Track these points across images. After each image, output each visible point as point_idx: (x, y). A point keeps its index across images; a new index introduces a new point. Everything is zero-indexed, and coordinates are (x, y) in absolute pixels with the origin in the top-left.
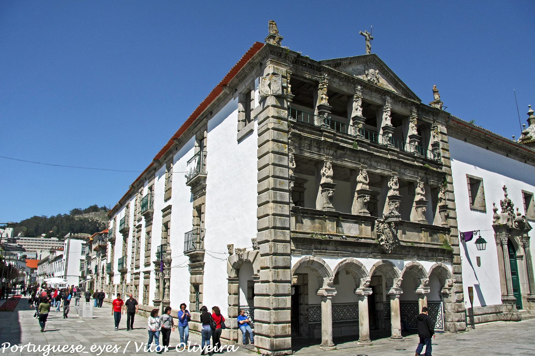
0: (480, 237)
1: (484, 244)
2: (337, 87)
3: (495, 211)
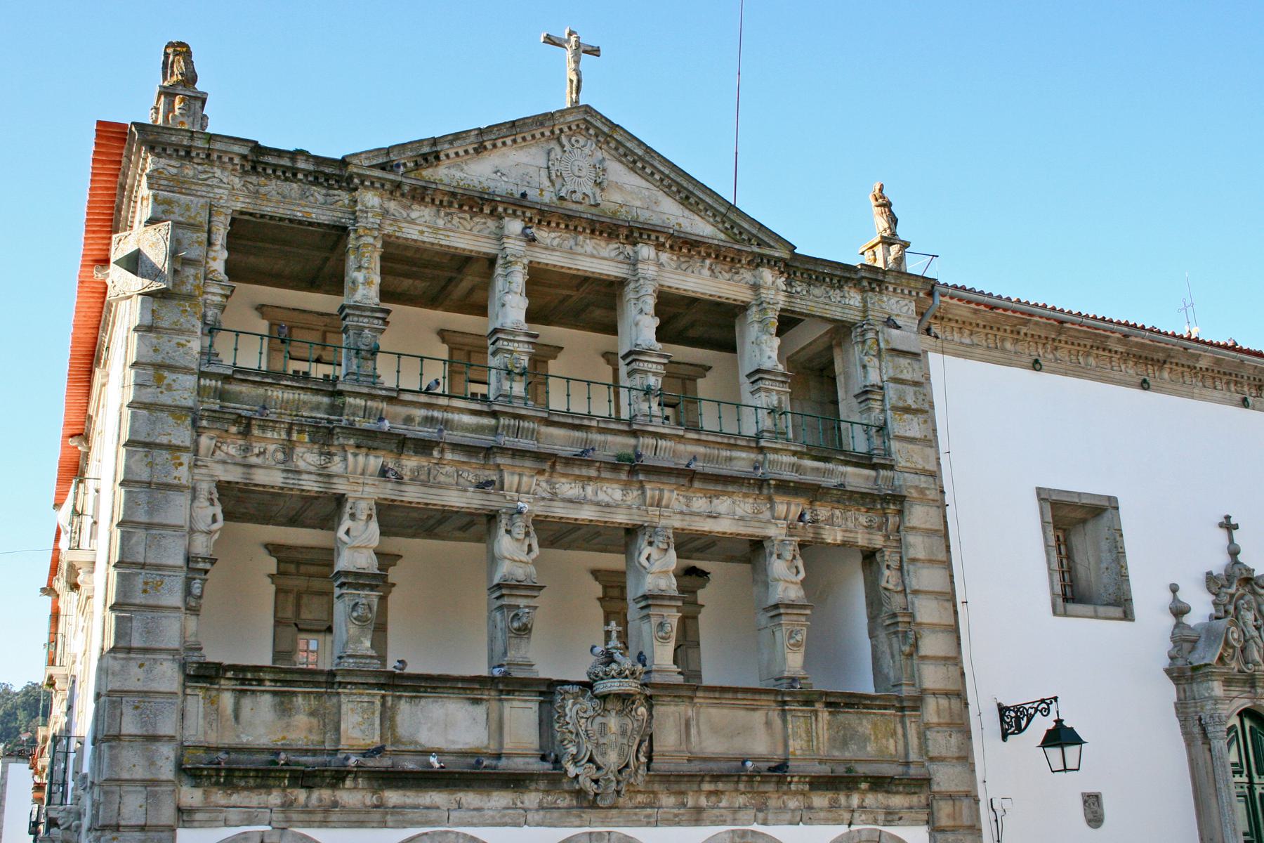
0: (1059, 722)
1: (1072, 751)
2: (427, 238)
3: (1179, 611)
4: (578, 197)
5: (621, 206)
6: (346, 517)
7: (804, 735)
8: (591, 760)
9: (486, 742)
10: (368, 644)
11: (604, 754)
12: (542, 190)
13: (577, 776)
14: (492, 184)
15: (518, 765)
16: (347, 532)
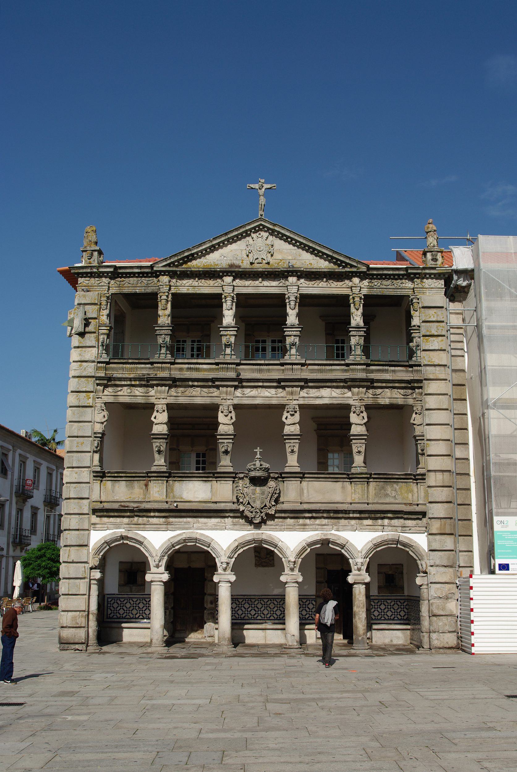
4: (260, 260)
5: (281, 260)
6: (155, 411)
7: (360, 492)
8: (249, 503)
9: (210, 497)
10: (163, 461)
11: (254, 502)
12: (243, 260)
13: (243, 511)
14: (219, 262)
15: (222, 506)
16: (155, 418)
